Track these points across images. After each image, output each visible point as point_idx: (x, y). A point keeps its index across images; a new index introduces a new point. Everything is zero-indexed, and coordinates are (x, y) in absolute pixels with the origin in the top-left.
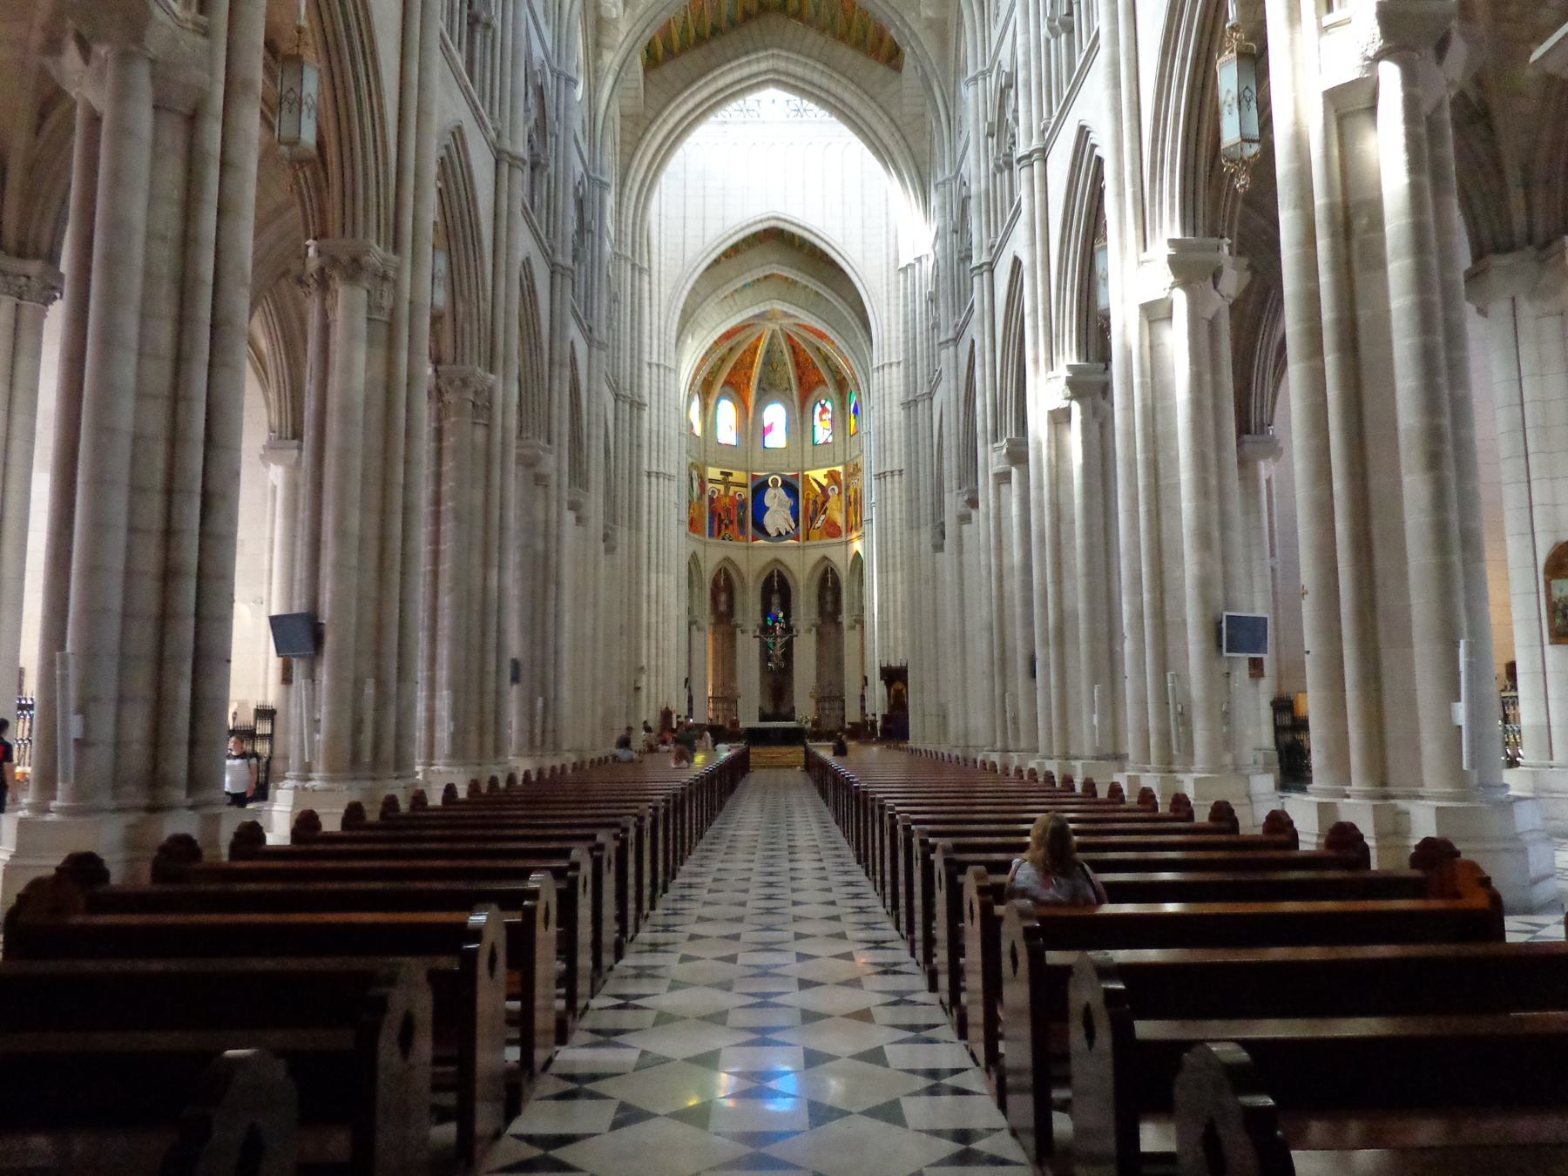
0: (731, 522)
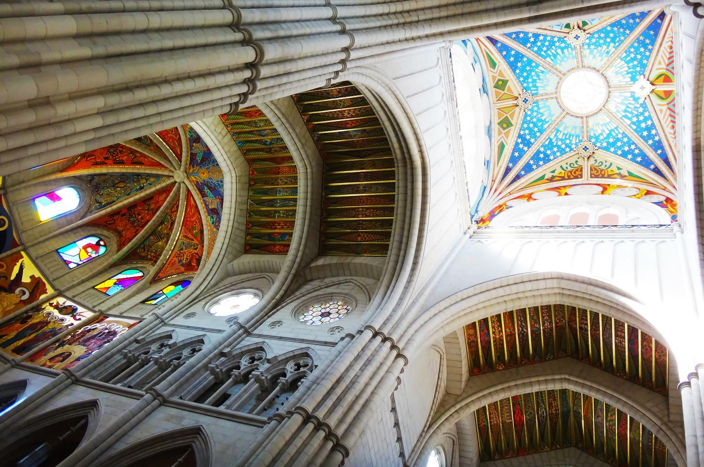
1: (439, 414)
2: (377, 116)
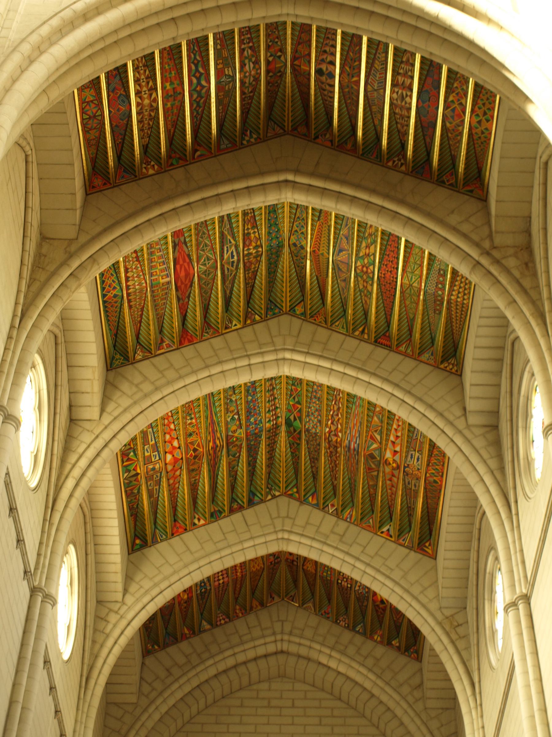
1: (34, 288)
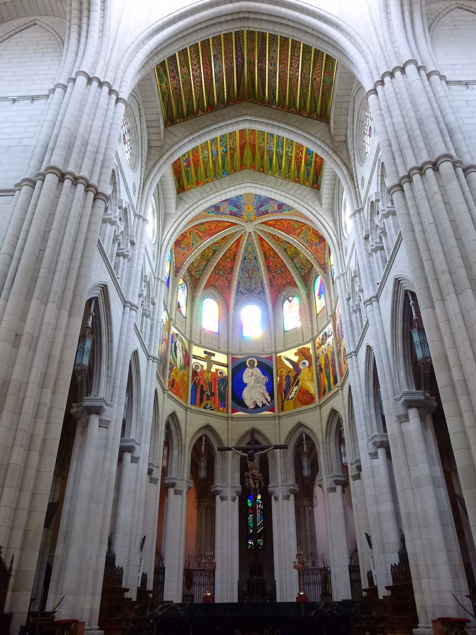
0: (213, 394)
2: (222, 34)
